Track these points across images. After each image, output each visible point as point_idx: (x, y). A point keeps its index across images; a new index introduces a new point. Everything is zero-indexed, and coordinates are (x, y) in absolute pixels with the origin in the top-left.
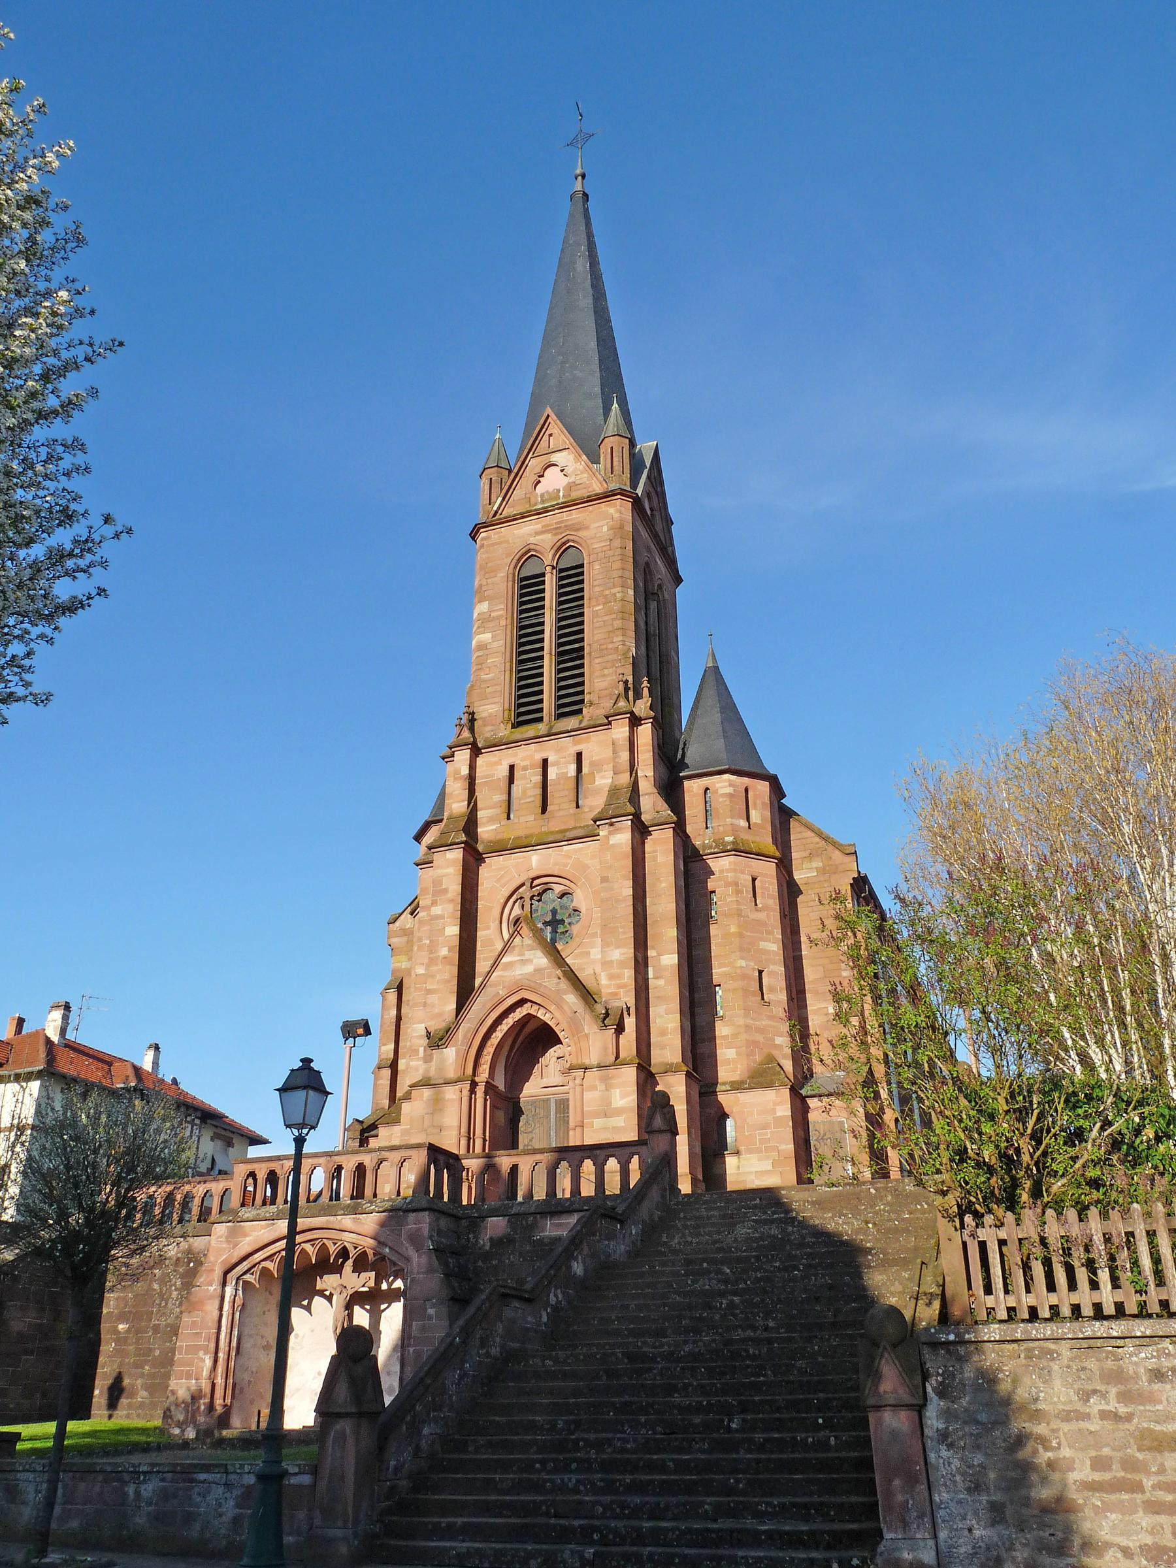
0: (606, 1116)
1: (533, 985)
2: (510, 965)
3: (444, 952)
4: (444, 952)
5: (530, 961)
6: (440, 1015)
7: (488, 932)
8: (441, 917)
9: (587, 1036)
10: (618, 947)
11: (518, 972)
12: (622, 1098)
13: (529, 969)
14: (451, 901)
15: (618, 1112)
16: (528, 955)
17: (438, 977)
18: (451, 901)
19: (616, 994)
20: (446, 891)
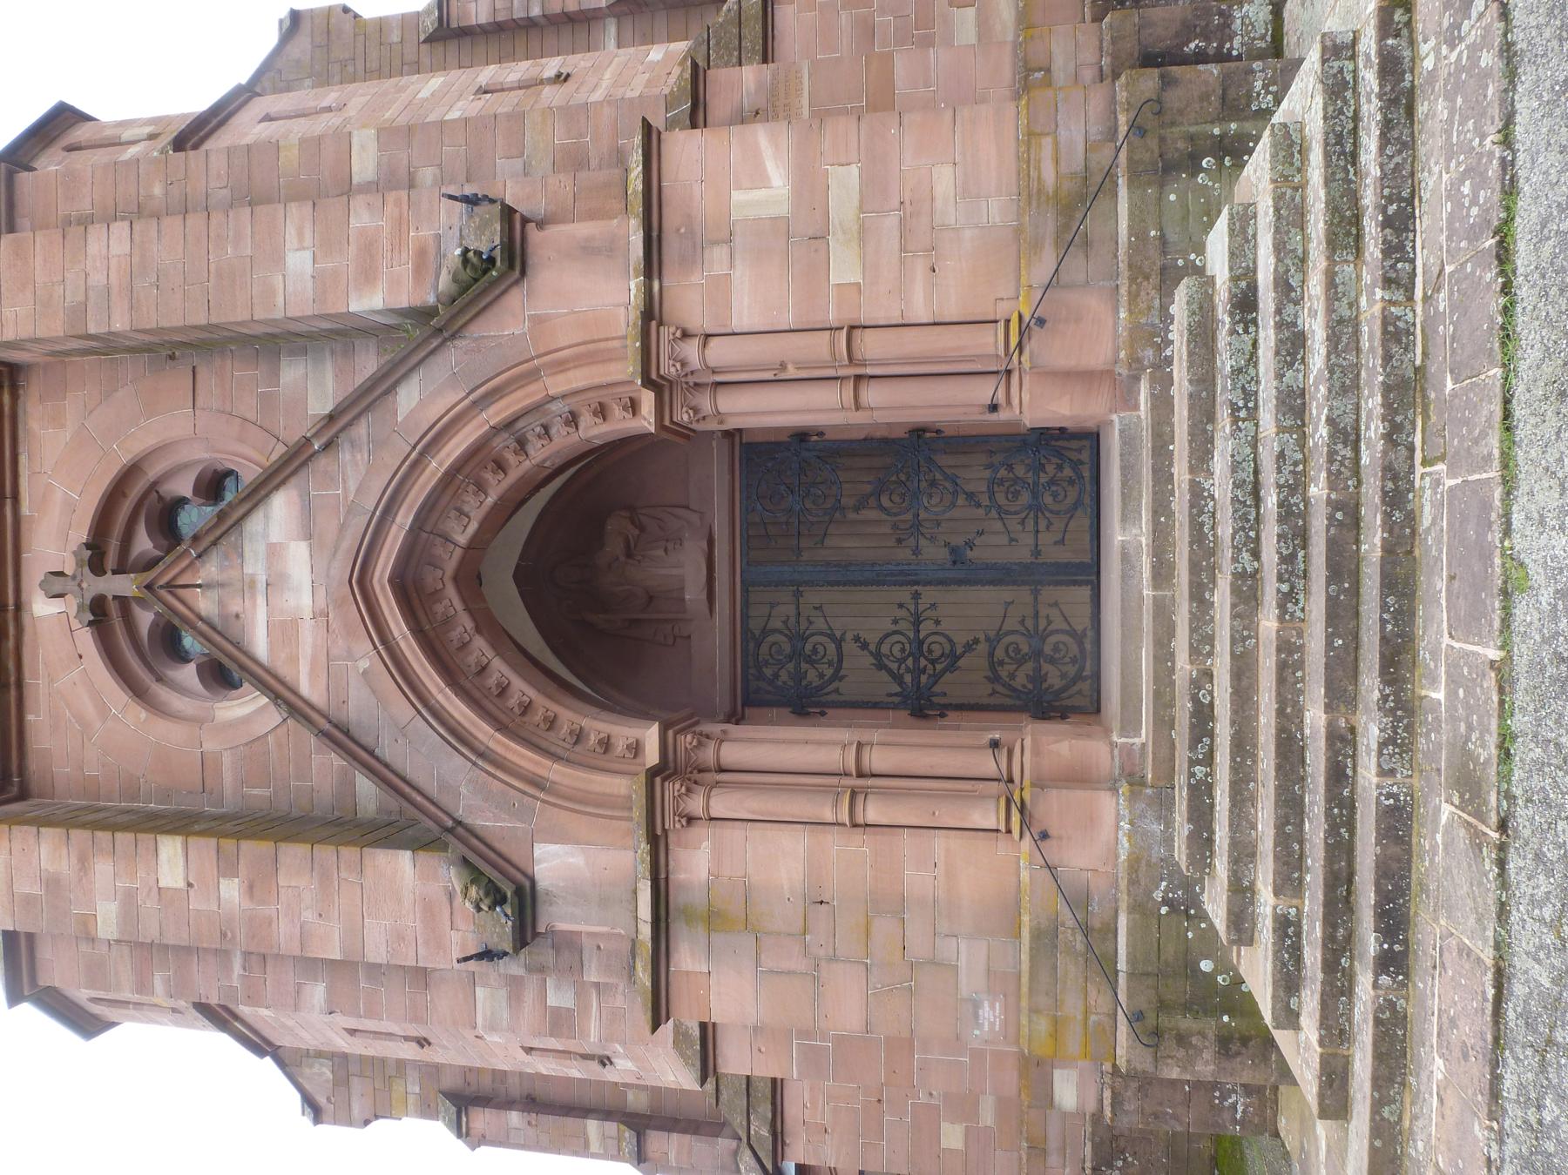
0: (820, 237)
1: (349, 542)
2: (284, 630)
3: (231, 890)
4: (231, 890)
5: (274, 552)
6: (428, 909)
7: (227, 759)
8: (129, 904)
9: (538, 321)
10: (279, 260)
11: (306, 600)
12: (759, 179)
13: (298, 557)
14: (84, 862)
15: (810, 187)
16: (255, 566)
17: (309, 915)
18: (84, 862)
19: (421, 253)
20: (53, 884)
